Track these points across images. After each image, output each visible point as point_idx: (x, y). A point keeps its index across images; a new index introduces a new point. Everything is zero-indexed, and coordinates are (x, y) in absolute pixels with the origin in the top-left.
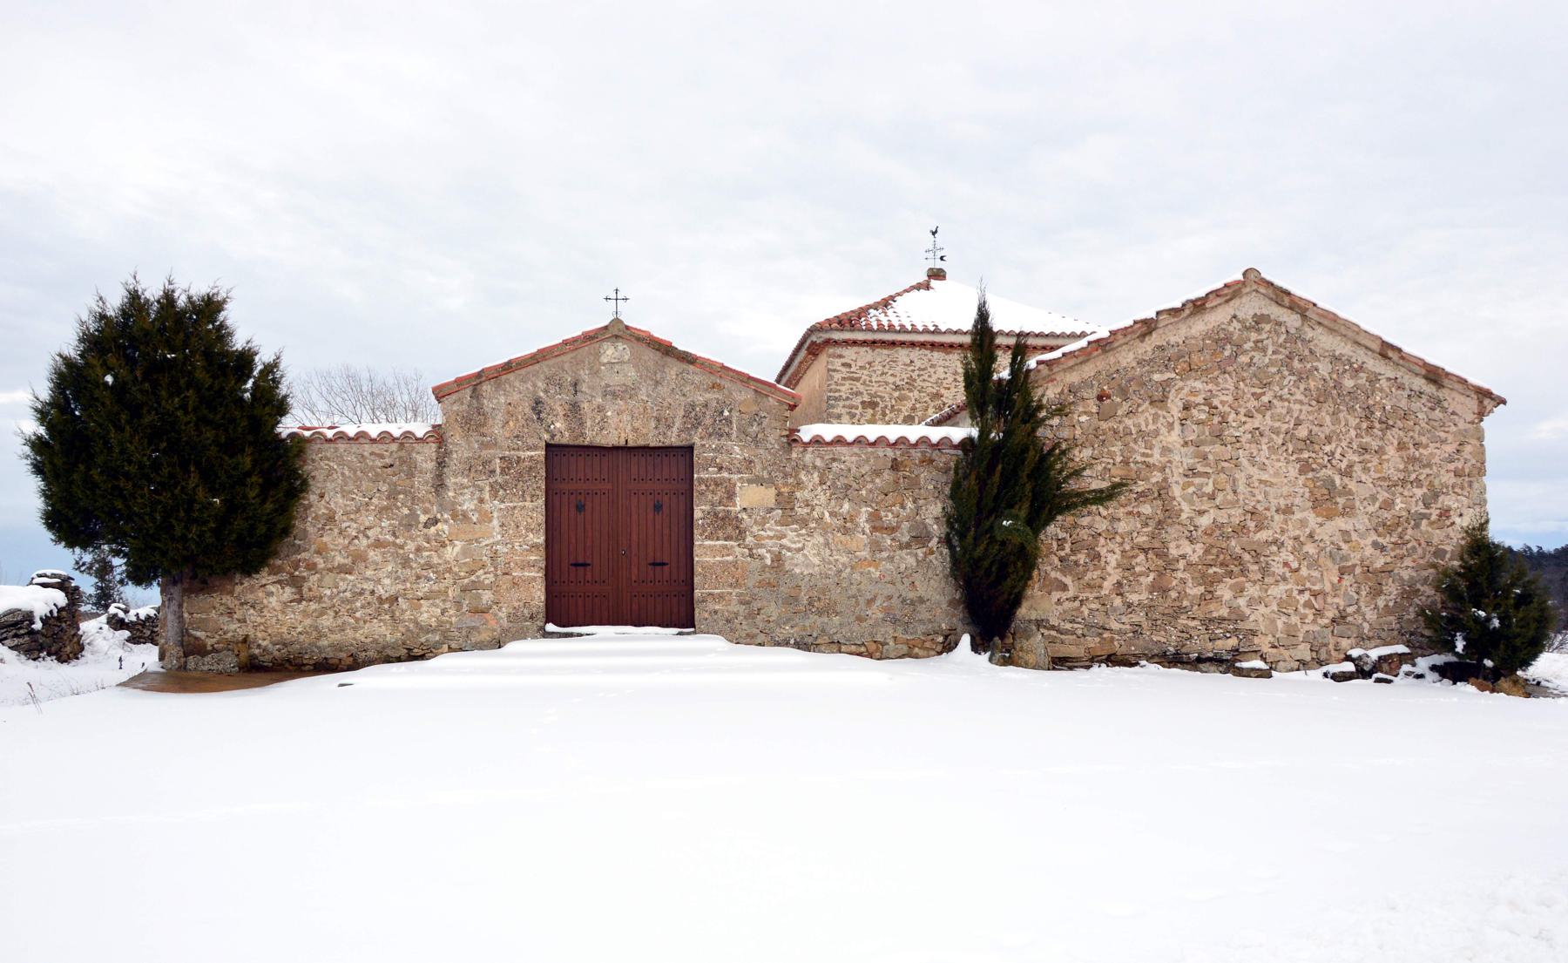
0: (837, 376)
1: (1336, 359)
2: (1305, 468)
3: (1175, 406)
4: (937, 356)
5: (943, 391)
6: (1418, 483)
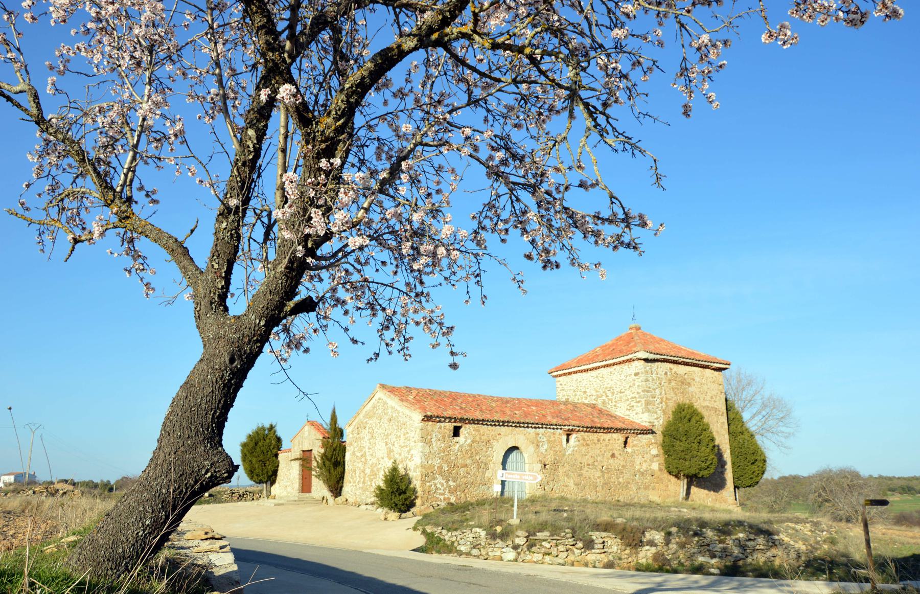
1: (393, 408)
2: (386, 445)
3: (367, 428)
4: (584, 374)
5: (587, 390)
6: (406, 446)
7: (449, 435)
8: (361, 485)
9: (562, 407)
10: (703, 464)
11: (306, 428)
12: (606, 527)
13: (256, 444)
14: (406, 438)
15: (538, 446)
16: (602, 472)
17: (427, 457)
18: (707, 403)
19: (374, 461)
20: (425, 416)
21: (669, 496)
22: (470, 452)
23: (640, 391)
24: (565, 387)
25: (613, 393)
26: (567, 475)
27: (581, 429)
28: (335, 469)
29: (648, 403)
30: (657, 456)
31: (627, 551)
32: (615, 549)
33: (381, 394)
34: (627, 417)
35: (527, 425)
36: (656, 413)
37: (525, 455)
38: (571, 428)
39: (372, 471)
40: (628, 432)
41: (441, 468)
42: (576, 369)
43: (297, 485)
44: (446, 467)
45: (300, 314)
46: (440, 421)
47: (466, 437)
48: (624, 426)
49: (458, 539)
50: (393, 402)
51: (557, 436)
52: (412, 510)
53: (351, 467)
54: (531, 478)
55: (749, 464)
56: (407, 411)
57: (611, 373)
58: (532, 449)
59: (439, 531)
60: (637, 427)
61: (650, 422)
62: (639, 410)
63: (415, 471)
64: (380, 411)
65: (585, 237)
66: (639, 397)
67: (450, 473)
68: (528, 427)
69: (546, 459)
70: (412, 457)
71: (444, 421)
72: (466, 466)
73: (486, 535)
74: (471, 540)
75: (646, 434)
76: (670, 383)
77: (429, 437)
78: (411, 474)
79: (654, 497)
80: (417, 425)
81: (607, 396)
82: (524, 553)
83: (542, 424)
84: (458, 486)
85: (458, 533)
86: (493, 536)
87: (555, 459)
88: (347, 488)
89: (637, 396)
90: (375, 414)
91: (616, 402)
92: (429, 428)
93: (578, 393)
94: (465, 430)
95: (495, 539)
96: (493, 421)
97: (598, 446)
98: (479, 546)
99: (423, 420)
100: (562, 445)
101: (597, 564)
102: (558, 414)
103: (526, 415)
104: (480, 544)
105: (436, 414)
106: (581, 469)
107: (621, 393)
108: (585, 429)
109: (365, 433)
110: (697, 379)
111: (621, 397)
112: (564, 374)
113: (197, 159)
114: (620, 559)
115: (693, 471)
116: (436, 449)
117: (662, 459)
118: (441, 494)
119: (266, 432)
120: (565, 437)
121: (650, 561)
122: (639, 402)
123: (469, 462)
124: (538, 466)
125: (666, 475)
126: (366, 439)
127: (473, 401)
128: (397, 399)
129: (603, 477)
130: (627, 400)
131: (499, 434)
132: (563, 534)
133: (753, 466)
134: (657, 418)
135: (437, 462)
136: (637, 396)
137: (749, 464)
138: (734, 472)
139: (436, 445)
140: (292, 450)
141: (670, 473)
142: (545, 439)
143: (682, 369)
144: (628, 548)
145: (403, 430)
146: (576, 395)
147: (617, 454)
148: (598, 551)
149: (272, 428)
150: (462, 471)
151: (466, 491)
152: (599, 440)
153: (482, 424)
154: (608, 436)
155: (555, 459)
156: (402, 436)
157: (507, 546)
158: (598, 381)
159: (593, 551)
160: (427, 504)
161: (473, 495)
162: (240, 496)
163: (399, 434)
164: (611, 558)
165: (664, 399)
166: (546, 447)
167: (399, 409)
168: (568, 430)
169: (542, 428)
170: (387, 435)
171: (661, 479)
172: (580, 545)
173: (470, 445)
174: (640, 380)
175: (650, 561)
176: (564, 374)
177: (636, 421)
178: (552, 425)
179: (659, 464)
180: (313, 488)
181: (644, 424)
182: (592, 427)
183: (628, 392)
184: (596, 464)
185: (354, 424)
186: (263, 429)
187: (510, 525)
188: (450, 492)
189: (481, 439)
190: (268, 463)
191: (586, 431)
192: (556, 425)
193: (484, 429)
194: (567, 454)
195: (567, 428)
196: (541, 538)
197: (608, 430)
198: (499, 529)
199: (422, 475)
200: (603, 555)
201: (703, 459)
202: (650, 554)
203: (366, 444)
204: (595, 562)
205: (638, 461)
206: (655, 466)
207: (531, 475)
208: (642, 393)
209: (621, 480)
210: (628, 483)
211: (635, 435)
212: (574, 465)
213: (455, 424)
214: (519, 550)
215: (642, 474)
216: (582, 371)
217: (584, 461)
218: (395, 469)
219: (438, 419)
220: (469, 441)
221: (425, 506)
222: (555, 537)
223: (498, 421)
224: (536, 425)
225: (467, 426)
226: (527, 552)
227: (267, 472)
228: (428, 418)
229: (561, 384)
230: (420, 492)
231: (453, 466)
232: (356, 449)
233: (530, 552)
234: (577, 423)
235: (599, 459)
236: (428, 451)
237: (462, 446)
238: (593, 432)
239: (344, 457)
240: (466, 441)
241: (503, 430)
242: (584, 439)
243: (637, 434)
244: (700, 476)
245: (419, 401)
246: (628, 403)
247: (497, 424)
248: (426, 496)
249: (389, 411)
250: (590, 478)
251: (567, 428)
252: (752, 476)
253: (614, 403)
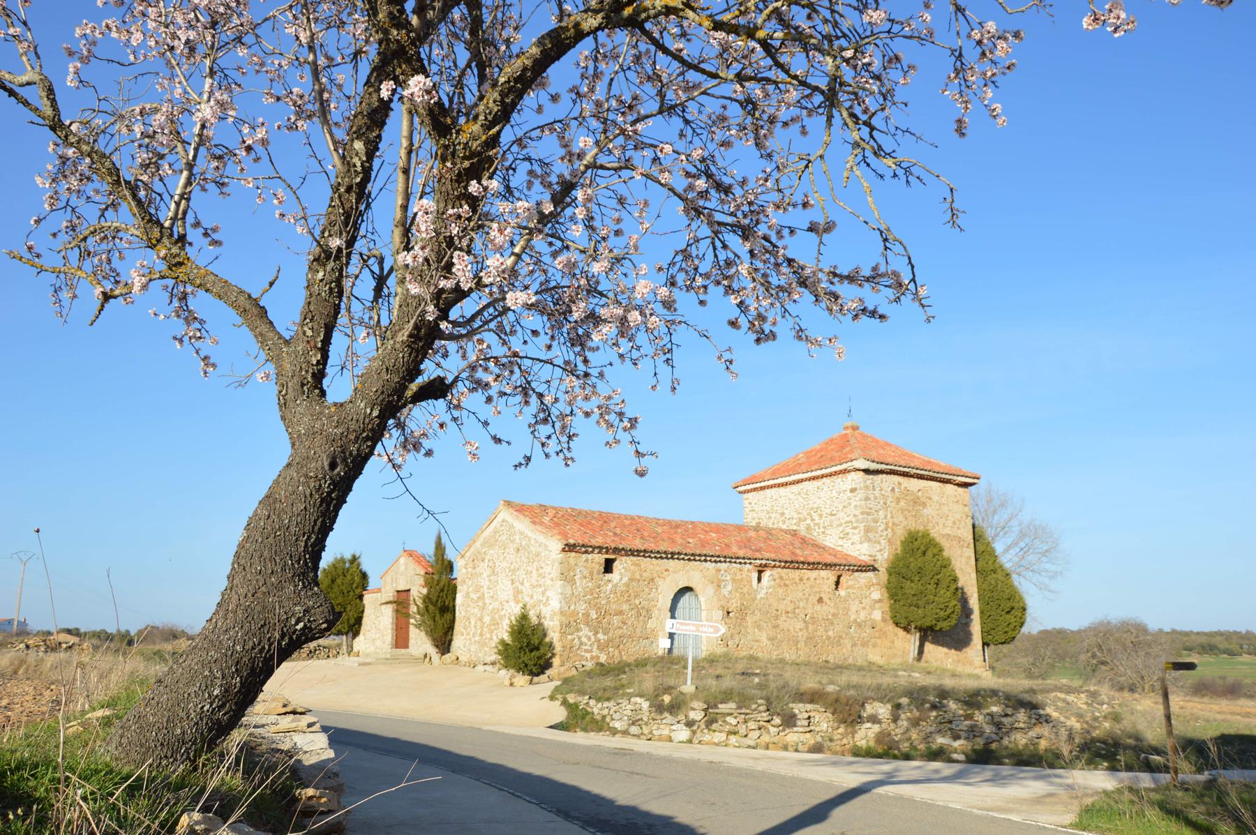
0: (747, 510)
1: (521, 533)
2: (513, 583)
3: (486, 561)
4: (782, 490)
6: (540, 586)
7: (599, 571)
8: (477, 638)
9: (752, 534)
10: (942, 613)
11: (402, 560)
12: (813, 697)
13: (333, 581)
14: (540, 575)
15: (719, 586)
16: (805, 622)
17: (567, 600)
18: (947, 531)
19: (496, 605)
20: (566, 545)
21: (894, 656)
22: (627, 593)
23: (858, 513)
24: (756, 508)
25: (821, 516)
26: (759, 627)
27: (778, 564)
28: (442, 616)
29: (867, 530)
30: (880, 601)
31: (841, 730)
32: (824, 726)
33: (505, 515)
34: (839, 549)
35: (705, 558)
36: (879, 543)
37: (702, 599)
38: (764, 562)
39: (493, 619)
40: (841, 568)
41: (587, 615)
42: (771, 482)
43: (389, 636)
44: (594, 615)
45: (423, 403)
46: (586, 552)
47: (621, 574)
48: (835, 561)
49: (611, 712)
50: (522, 525)
51: (745, 573)
52: (548, 672)
53: (463, 614)
54: (712, 630)
55: (1003, 613)
56: (541, 538)
57: (818, 488)
58: (710, 590)
59: (585, 702)
60: (853, 562)
61: (871, 556)
62: (856, 538)
63: (552, 620)
64: (504, 538)
65: (817, 300)
66: (857, 521)
67: (600, 622)
68: (705, 561)
69: (729, 605)
70: (547, 600)
71: (592, 552)
72: (621, 613)
73: (650, 707)
74: (629, 713)
75: (865, 571)
76: (898, 503)
77: (572, 574)
78: (547, 623)
79: (875, 657)
80: (554, 556)
81: (813, 520)
82: (702, 731)
83: (725, 557)
84: (611, 640)
85: (611, 704)
86: (659, 708)
87: (743, 604)
88: (458, 642)
89: (854, 520)
90: (497, 541)
91: (824, 527)
92: (572, 561)
93: (773, 515)
95: (661, 713)
96: (658, 552)
97: (801, 587)
98: (640, 722)
99: (563, 550)
100: (751, 586)
101: (800, 747)
102: (746, 543)
103: (703, 544)
104: (641, 719)
105: (581, 542)
106: (777, 617)
107: (832, 515)
108: (783, 564)
109: (483, 568)
110: (935, 498)
111: (831, 522)
112: (755, 490)
113: (284, 181)
114: (831, 740)
115: (928, 622)
116: (580, 590)
117: (886, 605)
118: (587, 651)
119: (347, 565)
120: (755, 575)
121: (872, 744)
122: (855, 528)
123: (625, 607)
124: (719, 614)
125: (891, 627)
126: (485, 575)
127: (631, 525)
128: (527, 521)
129: (807, 628)
130: (841, 525)
131: (667, 570)
132: (754, 706)
133: (1008, 616)
134: (881, 550)
135: (582, 608)
136: (854, 520)
137: (1003, 613)
138: (983, 623)
139: (581, 584)
140: (383, 590)
141: (897, 624)
142: (728, 578)
144: (842, 726)
145: (535, 563)
146: (770, 518)
147: (825, 599)
148: (801, 729)
149: (354, 559)
150: (616, 620)
151: (621, 647)
152: (801, 580)
153: (644, 556)
154: (815, 574)
155: (743, 604)
156: (534, 571)
157: (678, 722)
158: (801, 499)
159: (795, 729)
160: (568, 665)
161: (631, 652)
162: (311, 652)
163: (529, 569)
164: (819, 739)
165: (890, 525)
166: (729, 588)
167: (530, 534)
168: (761, 565)
169: (725, 562)
170: (514, 571)
171: (885, 633)
172: (777, 721)
173: (627, 585)
174: (857, 499)
175: (872, 744)
176: (755, 490)
177: (852, 554)
178: (738, 558)
179: (883, 613)
180: (412, 642)
181: (863, 558)
182: (792, 562)
183: (841, 515)
184: (797, 611)
185: (468, 554)
186: (343, 560)
187: (682, 693)
188: (601, 648)
189: (641, 576)
190: (349, 607)
191: (784, 567)
192: (744, 558)
193: (645, 562)
194: (759, 597)
195: (758, 562)
196: (724, 711)
197: (814, 566)
198: (667, 699)
199: (562, 625)
200: (808, 735)
201: (942, 606)
202: (871, 734)
203: (484, 582)
204: (797, 744)
205: (854, 607)
206: (877, 615)
207: (712, 627)
208: (860, 516)
209: (830, 633)
210: (841, 637)
211: (850, 573)
212: (768, 612)
213: (607, 556)
214: (695, 728)
215: (859, 625)
216: (779, 485)
217: (781, 607)
218: (524, 617)
219: (583, 549)
220: (625, 579)
221: (566, 667)
222: (743, 711)
223: (665, 552)
224: (717, 558)
225: (624, 558)
226: (706, 731)
227: (348, 620)
228: (570, 548)
229: (750, 503)
230: (558, 648)
231: (604, 614)
232: (470, 589)
233: (709, 730)
234: (773, 556)
235: (801, 604)
236: (570, 592)
237: (615, 586)
238: (794, 568)
239: (454, 599)
240: (621, 579)
241: (672, 564)
242: (781, 578)
243: (853, 571)
244: (937, 629)
245: (557, 525)
246: (841, 529)
247: (664, 556)
248: (566, 653)
249: (517, 537)
250: (789, 630)
251: (758, 562)
252: (1007, 629)
253: (822, 530)
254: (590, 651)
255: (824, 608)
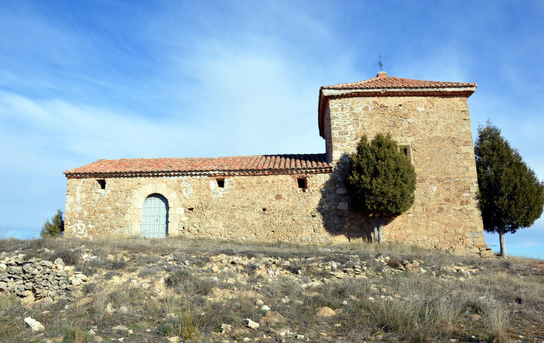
26: (215, 218)
35: (168, 174)
41: (81, 214)
44: (86, 213)
51: (203, 181)
94: (109, 181)
118: (80, 235)
131: (139, 184)
135: (79, 209)
143: (391, 102)
147: (284, 195)
152: (259, 183)
242: (239, 183)
254: (83, 235)
255: (282, 203)
